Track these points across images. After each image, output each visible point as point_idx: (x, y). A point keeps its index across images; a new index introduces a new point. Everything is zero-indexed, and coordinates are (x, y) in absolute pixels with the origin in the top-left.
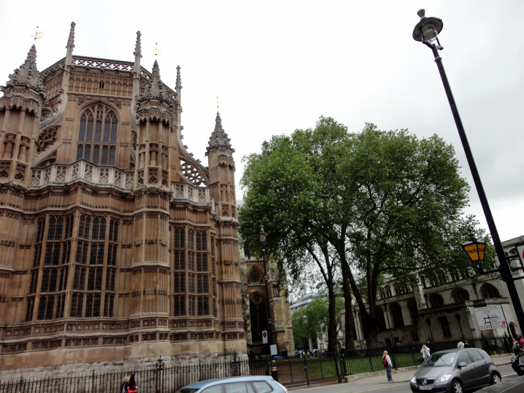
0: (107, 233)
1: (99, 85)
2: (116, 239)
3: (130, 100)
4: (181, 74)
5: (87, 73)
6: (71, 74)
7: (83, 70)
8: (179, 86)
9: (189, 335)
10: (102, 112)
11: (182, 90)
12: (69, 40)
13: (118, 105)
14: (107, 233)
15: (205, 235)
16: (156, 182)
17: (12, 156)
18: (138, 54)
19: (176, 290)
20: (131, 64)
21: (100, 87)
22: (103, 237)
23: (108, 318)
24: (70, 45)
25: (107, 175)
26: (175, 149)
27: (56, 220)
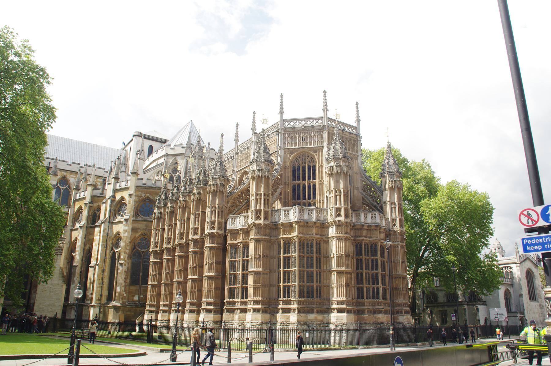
0: (315, 250)
1: (301, 139)
2: (320, 253)
3: (323, 147)
4: (359, 109)
5: (294, 131)
6: (284, 134)
7: (291, 130)
8: (358, 121)
9: (366, 311)
10: (305, 159)
11: (360, 122)
12: (281, 108)
13: (315, 152)
14: (315, 250)
15: (376, 245)
16: (341, 217)
17: (261, 207)
18: (325, 109)
19: (358, 283)
20: (321, 118)
21: (303, 140)
22: (312, 253)
23: (318, 300)
24: (282, 113)
25: (311, 213)
26: (358, 174)
27: (287, 243)
